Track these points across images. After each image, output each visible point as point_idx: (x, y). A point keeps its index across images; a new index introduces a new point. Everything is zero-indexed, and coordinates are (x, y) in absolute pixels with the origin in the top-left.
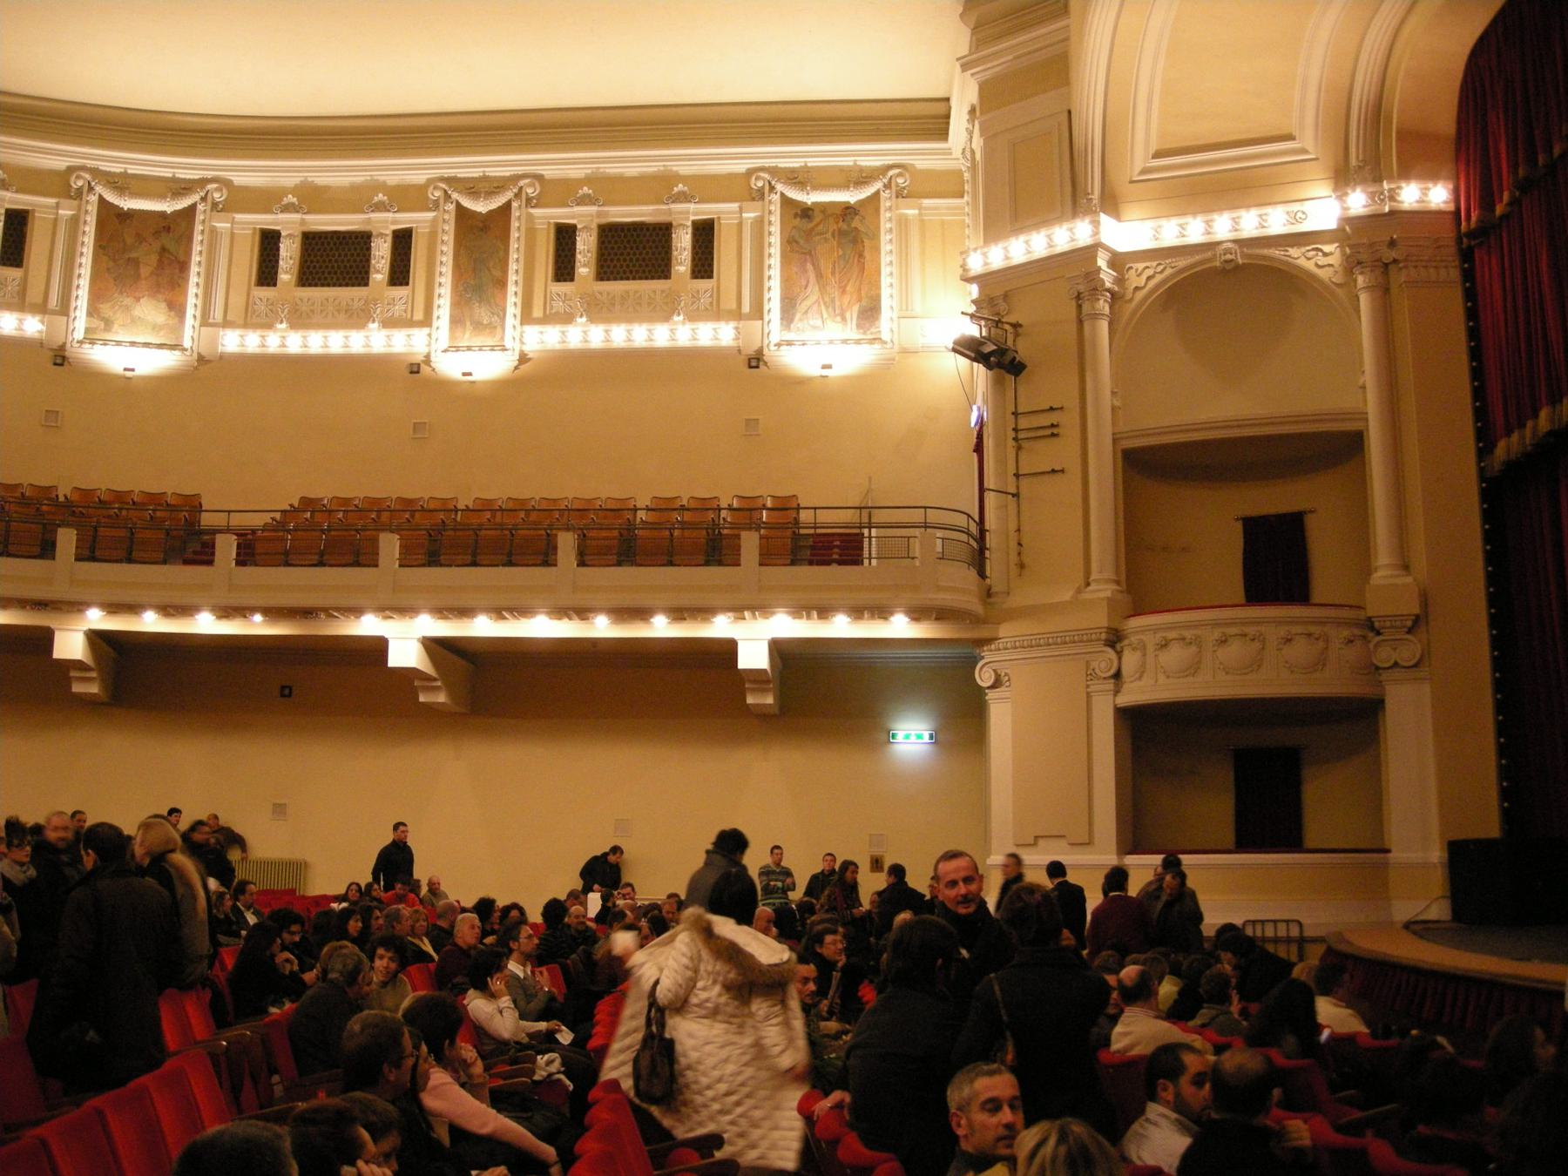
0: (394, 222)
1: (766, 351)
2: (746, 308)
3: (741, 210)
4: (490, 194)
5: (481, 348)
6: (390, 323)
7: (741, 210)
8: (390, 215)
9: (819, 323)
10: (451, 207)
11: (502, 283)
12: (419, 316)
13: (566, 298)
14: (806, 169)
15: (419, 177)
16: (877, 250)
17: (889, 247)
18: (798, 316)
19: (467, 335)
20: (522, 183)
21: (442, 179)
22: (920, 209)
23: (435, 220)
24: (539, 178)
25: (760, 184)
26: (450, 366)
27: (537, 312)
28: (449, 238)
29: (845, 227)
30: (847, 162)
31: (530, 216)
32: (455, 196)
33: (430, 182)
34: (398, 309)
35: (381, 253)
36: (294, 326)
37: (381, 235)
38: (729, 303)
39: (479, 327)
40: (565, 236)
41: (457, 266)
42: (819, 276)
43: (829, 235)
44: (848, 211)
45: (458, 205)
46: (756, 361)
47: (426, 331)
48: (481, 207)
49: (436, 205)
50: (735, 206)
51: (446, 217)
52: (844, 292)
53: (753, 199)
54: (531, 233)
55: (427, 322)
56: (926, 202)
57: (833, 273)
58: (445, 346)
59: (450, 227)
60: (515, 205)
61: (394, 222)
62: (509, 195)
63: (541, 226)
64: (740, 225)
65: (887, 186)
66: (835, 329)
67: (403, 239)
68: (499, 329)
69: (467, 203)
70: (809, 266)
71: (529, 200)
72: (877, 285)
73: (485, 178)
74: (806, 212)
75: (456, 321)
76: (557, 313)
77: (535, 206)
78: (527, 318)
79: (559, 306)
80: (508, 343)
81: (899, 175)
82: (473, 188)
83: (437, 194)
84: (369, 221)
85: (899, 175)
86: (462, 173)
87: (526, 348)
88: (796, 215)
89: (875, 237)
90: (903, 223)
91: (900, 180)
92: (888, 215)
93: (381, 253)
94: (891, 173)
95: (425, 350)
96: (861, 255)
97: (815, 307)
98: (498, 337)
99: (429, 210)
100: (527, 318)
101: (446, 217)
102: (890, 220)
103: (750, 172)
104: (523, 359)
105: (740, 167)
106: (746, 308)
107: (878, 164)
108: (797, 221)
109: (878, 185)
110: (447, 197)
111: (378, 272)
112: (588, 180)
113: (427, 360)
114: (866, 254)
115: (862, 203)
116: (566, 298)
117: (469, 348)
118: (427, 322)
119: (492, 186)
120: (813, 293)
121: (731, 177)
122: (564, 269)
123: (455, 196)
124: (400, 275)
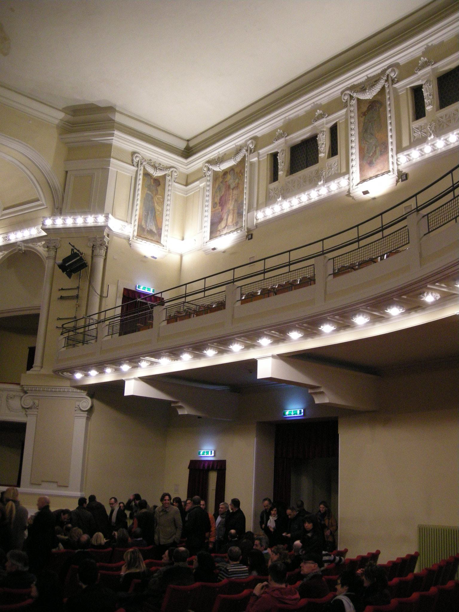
4: (373, 86)
10: (354, 102)
12: (344, 170)
13: (420, 128)
26: (358, 192)
31: (395, 90)
32: (355, 95)
33: (342, 93)
36: (285, 198)
40: (417, 92)
45: (358, 100)
47: (347, 177)
48: (368, 96)
49: (345, 105)
51: (352, 109)
54: (397, 98)
58: (359, 181)
61: (327, 123)
63: (402, 93)
71: (393, 80)
73: (369, 79)
77: (398, 82)
82: (362, 88)
83: (346, 98)
87: (400, 168)
95: (347, 188)
110: (351, 97)
118: (347, 172)
119: (372, 82)
123: (355, 95)
124: (333, 151)
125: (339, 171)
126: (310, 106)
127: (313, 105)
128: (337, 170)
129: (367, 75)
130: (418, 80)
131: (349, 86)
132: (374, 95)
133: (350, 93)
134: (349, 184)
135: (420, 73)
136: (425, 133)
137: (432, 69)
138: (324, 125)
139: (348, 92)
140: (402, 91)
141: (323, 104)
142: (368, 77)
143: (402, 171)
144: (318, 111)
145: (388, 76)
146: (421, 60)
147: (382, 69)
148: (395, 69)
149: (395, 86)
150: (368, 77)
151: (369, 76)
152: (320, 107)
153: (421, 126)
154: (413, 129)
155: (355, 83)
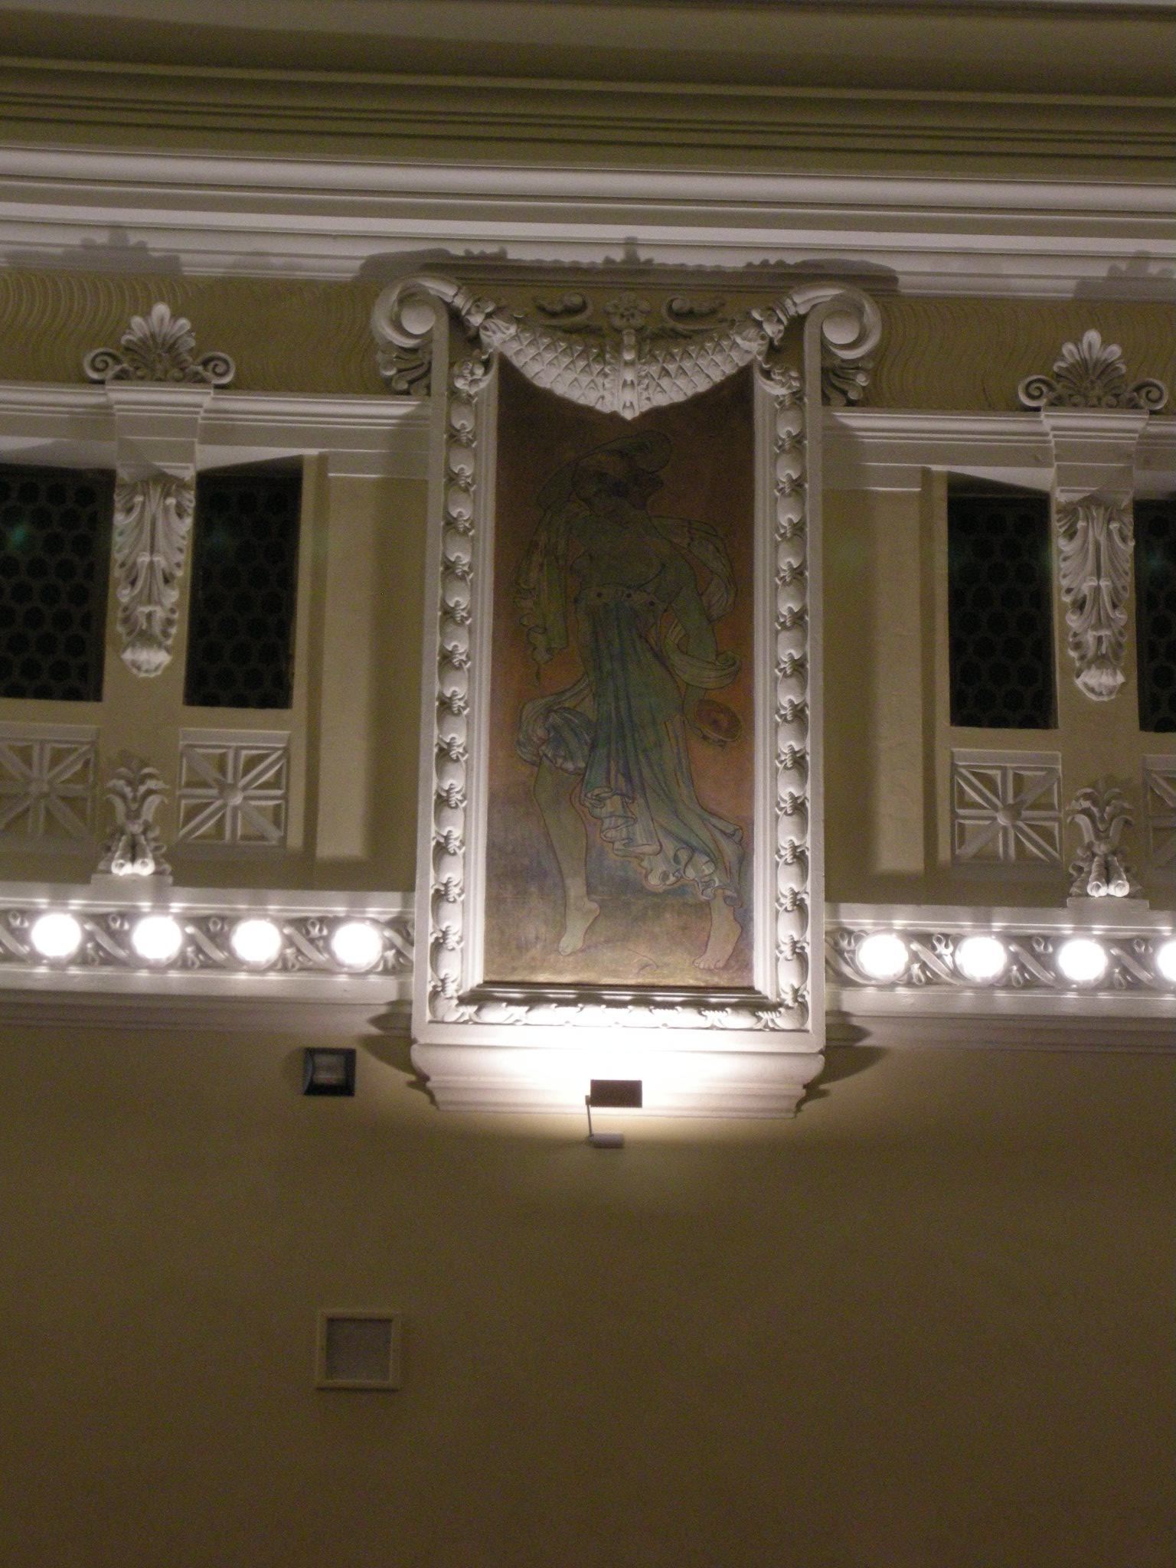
0: (220, 432)
5: (644, 996)
6: (216, 867)
8: (203, 399)
10: (479, 382)
11: (728, 723)
12: (343, 838)
15: (327, 244)
19: (572, 940)
20: (800, 301)
21: (440, 264)
23: (406, 432)
24: (876, 283)
27: (897, 850)
28: (476, 509)
31: (842, 440)
32: (501, 337)
33: (379, 272)
34: (244, 805)
35: (154, 554)
37: (167, 483)
39: (625, 904)
40: (995, 539)
41: (514, 637)
45: (514, 387)
47: (384, 906)
48: (622, 391)
49: (414, 372)
54: (847, 509)
55: (387, 863)
58: (475, 977)
59: (478, 466)
60: (770, 390)
62: (748, 347)
67: (252, 518)
68: (722, 920)
69: (557, 373)
71: (835, 378)
73: (632, 274)
75: (512, 877)
76: (985, 859)
77: (866, 402)
78: (852, 873)
79: (993, 828)
80: (772, 973)
82: (580, 307)
83: (418, 324)
84: (102, 419)
86: (528, 240)
93: (154, 554)
95: (386, 989)
98: (718, 951)
99: (386, 389)
100: (852, 873)
101: (463, 421)
104: (845, 1046)
110: (465, 339)
111: (146, 638)
112: (1089, 306)
113: (394, 1031)
116: (1023, 798)
117: (587, 994)
118: (387, 863)
122: (1000, 670)
123: (501, 337)
125: (296, 839)
126: (73, 239)
127: (101, 238)
128: (278, 817)
129: (631, 243)
130: (1037, 458)
131: (458, 250)
132: (661, 400)
133: (459, 302)
134: (398, 967)
135: (1050, 421)
136: (1047, 835)
137: (1145, 436)
138: (195, 426)
139: (447, 291)
140: (890, 477)
141: (187, 271)
142: (631, 259)
143: (860, 1033)
144: (161, 310)
145: (797, 323)
146: (1077, 341)
147: (756, 259)
148: (871, 314)
149: (856, 420)
150: (631, 259)
151: (643, 255)
152: (164, 279)
153: (1018, 779)
154: (954, 768)
155: (514, 254)
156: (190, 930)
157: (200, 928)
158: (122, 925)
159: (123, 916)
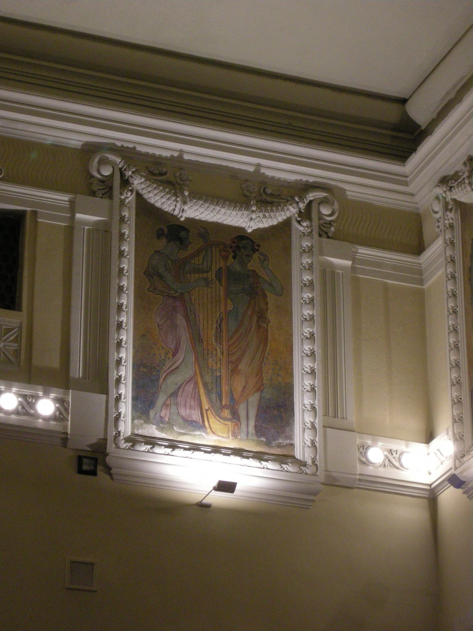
1: (111, 448)
2: (77, 369)
3: (72, 208)
7: (72, 208)
9: (196, 415)
14: (178, 161)
16: (286, 312)
17: (307, 312)
18: (161, 399)
22: (354, 260)
25: (106, 171)
29: (238, 268)
30: (244, 163)
38: (48, 357)
42: (197, 339)
43: (212, 276)
44: (240, 241)
46: (93, 460)
50: (63, 198)
52: (234, 371)
53: (93, 194)
56: (363, 251)
57: (218, 338)
64: (70, 231)
65: (306, 215)
66: (217, 434)
70: (180, 320)
72: (286, 368)
74: (176, 232)
81: (323, 201)
85: (323, 201)
88: (160, 234)
89: (284, 291)
90: (329, 276)
91: (325, 211)
92: (306, 260)
94: (311, 196)
96: (262, 316)
97: (190, 388)
102: (310, 267)
103: (90, 150)
105: (75, 136)
106: (77, 369)
107: (292, 178)
108: (161, 244)
109: (292, 211)
114: (270, 316)
115: (264, 234)
120: (183, 369)
121: (57, 151)
156: (20, 399)
157: (23, 398)
158: (32, 400)
159: (32, 396)
